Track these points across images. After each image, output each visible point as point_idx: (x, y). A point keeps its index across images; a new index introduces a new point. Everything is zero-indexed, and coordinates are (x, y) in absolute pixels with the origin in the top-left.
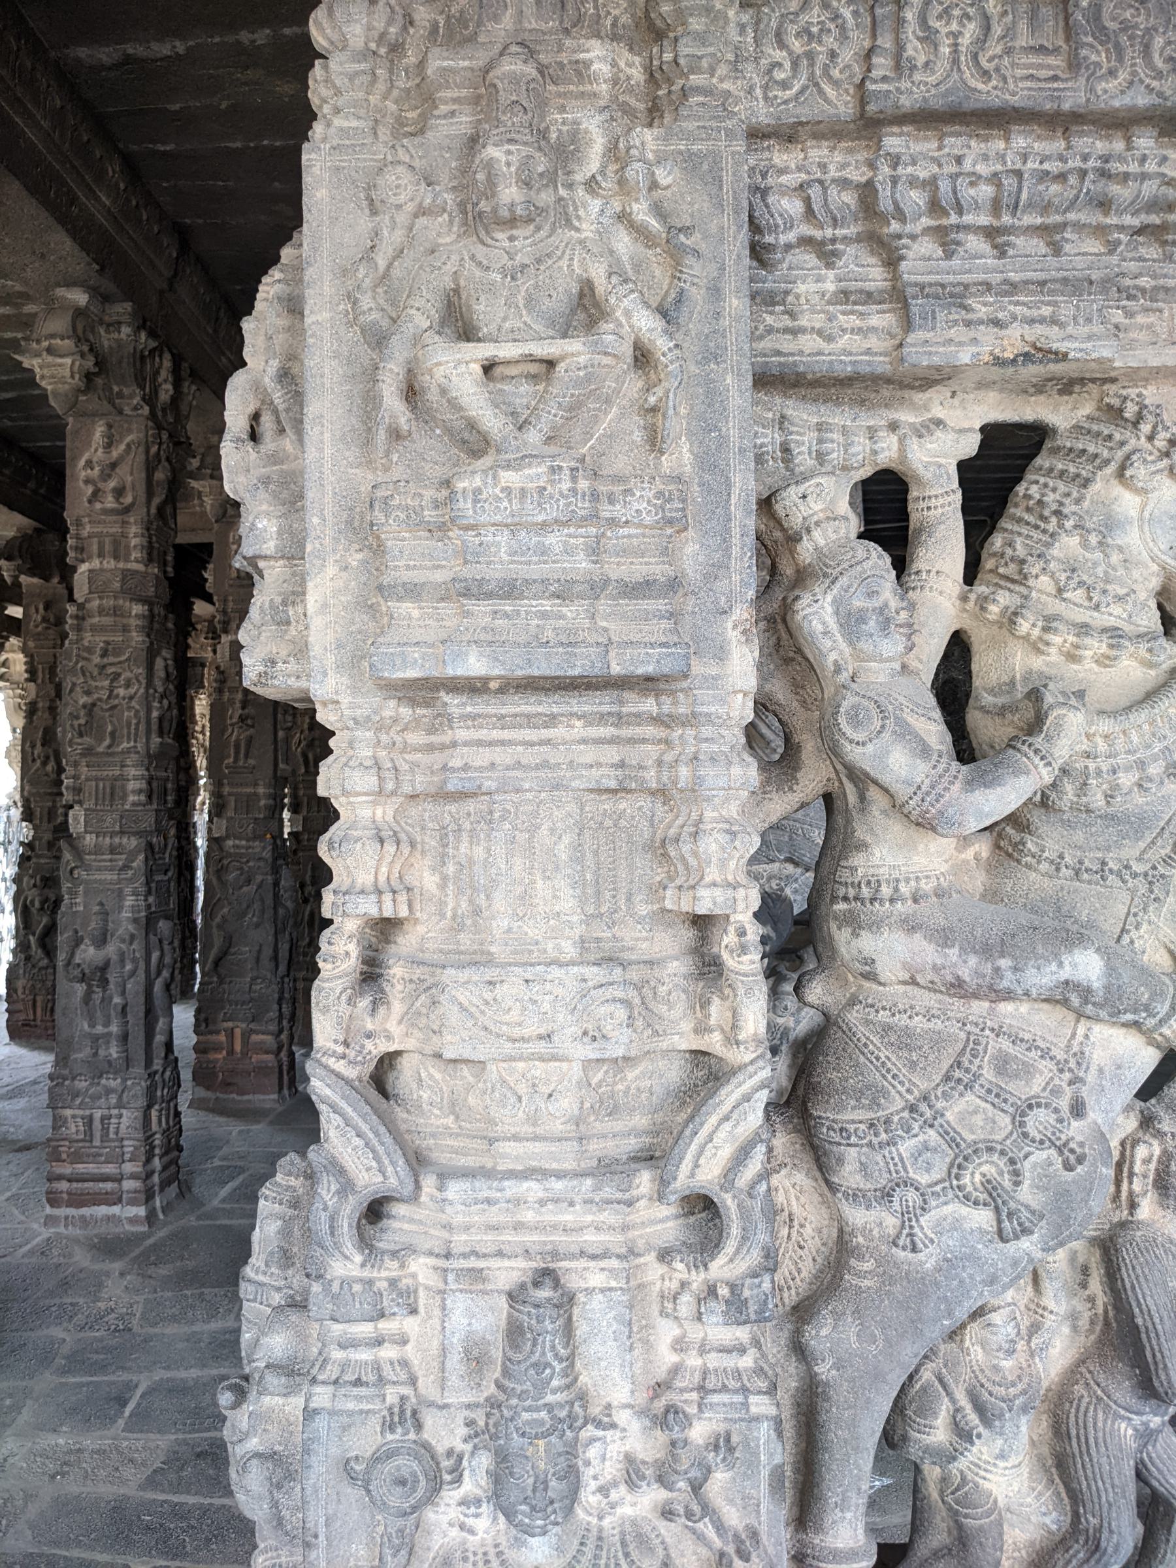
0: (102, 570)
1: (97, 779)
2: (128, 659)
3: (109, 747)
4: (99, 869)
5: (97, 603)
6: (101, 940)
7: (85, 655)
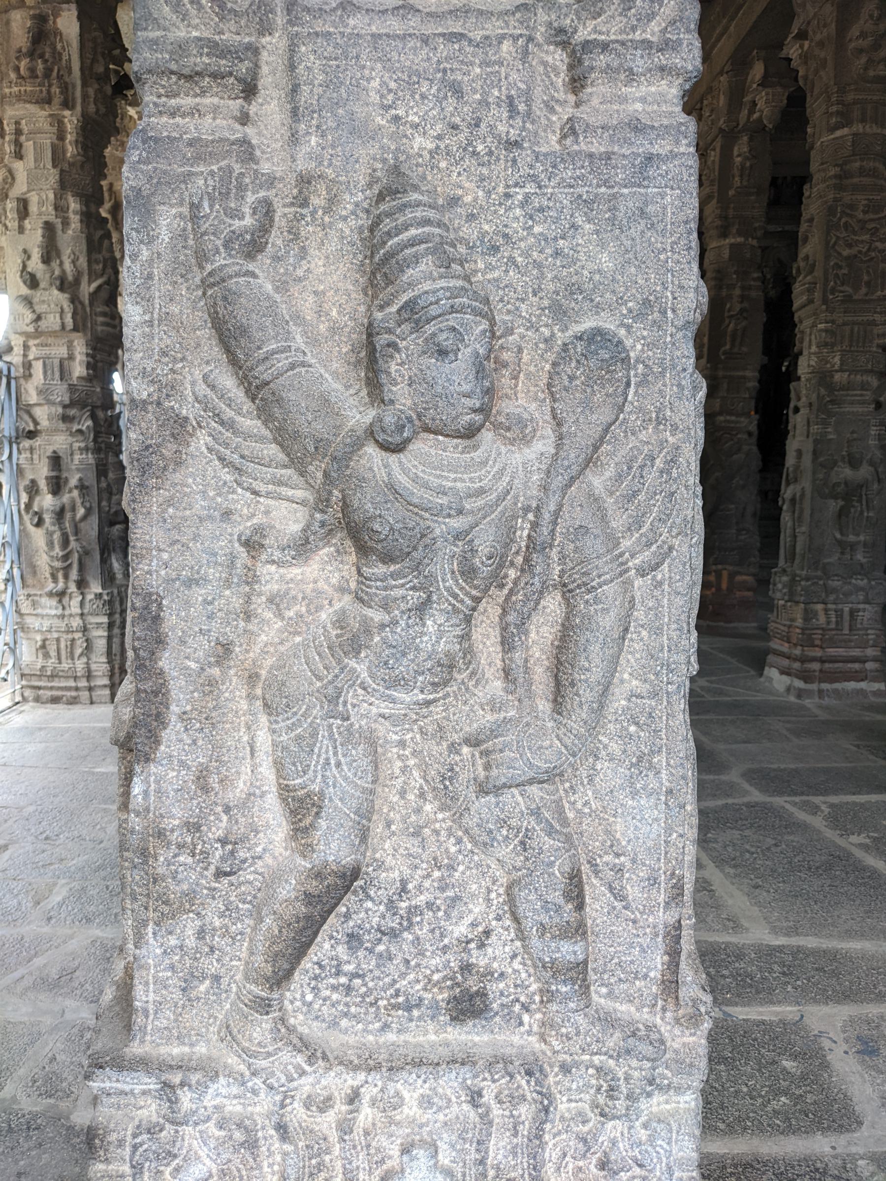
1: (854, 323)
3: (866, 295)
4: (852, 403)
5: (857, 164)
6: (854, 464)
7: (848, 211)
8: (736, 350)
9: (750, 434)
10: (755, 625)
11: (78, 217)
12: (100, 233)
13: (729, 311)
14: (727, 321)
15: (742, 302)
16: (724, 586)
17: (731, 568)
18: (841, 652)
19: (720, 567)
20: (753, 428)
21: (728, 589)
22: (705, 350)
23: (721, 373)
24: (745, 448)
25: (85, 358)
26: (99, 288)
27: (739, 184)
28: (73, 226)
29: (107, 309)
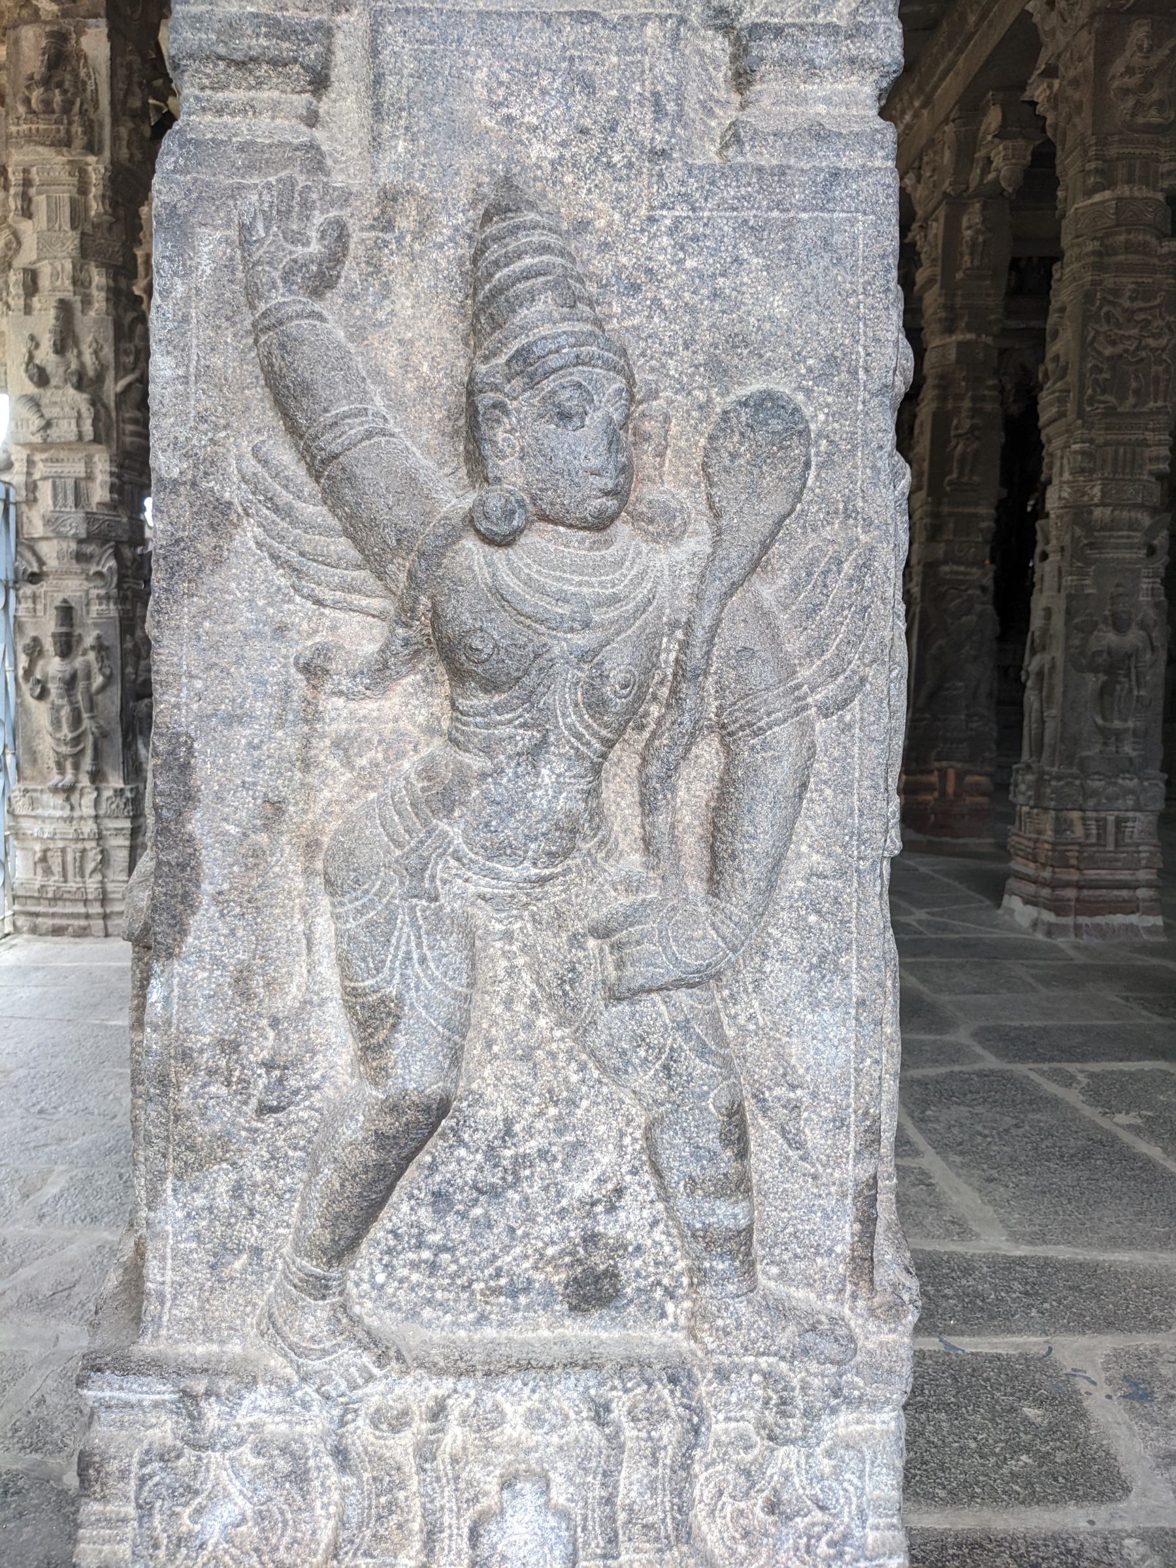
0: (1132, 198)
1: (1119, 443)
2: (1159, 305)
3: (1135, 406)
4: (1117, 547)
5: (1122, 238)
6: (1120, 625)
8: (965, 479)
9: (984, 589)
10: (991, 840)
11: (103, 294)
12: (130, 316)
13: (956, 428)
14: (953, 443)
15: (972, 417)
16: (950, 789)
17: (959, 765)
18: (1104, 874)
19: (944, 764)
20: (988, 581)
21: (955, 794)
22: (925, 478)
23: (946, 509)
24: (978, 607)
25: (107, 478)
26: (129, 387)
27: (969, 264)
28: (96, 305)
29: (138, 415)
